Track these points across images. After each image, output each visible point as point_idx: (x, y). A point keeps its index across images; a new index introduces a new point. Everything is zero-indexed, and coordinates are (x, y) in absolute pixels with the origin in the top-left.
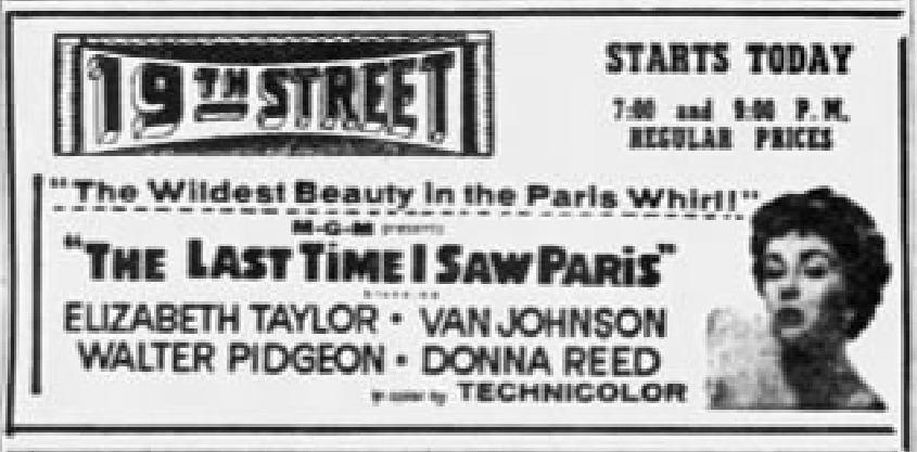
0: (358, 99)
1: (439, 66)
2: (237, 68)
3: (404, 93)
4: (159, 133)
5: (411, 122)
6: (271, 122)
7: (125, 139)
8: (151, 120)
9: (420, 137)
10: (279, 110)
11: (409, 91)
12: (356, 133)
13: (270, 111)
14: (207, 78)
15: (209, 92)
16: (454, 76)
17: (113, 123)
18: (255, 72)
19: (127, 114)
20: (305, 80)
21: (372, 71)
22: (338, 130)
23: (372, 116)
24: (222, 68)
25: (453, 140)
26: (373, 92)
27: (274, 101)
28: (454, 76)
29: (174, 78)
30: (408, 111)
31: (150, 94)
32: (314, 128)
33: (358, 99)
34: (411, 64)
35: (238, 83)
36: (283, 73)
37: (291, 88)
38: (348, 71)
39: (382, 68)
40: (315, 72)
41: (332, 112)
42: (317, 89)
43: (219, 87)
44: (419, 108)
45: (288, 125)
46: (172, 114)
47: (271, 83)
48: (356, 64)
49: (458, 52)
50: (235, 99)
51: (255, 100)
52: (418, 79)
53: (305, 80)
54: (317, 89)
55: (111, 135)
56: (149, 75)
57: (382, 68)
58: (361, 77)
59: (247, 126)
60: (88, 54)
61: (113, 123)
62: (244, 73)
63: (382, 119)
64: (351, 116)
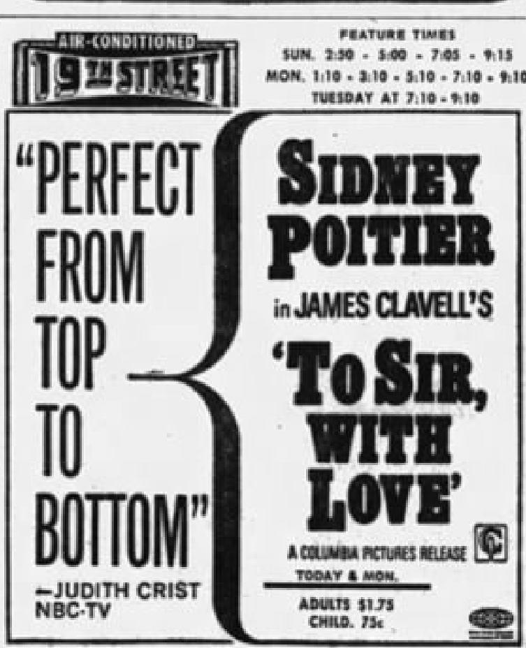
0: (171, 79)
1: (211, 60)
2: (107, 60)
3: (194, 74)
4: (67, 94)
5: (196, 90)
6: (124, 89)
7: (51, 97)
8: (64, 87)
9: (201, 98)
12: (167, 96)
13: (122, 84)
14: (92, 65)
16: (219, 66)
18: (115, 62)
19: (52, 85)
21: (177, 63)
22: (158, 93)
23: (177, 86)
24: (100, 60)
25: (218, 100)
28: (219, 66)
29: (76, 64)
31: (63, 73)
32: (146, 92)
35: (107, 69)
36: (129, 64)
37: (133, 71)
38: (164, 63)
40: (146, 63)
41: (155, 84)
42: (147, 73)
43: (98, 71)
44: (201, 83)
45: (133, 92)
46: (75, 85)
47: (124, 68)
48: (168, 58)
49: (220, 53)
50: (105, 77)
52: (201, 68)
53: (141, 66)
54: (147, 73)
55: (43, 96)
56: (63, 62)
59: (111, 91)
60: (32, 52)
61: (44, 88)
62: (110, 64)
64: (165, 86)
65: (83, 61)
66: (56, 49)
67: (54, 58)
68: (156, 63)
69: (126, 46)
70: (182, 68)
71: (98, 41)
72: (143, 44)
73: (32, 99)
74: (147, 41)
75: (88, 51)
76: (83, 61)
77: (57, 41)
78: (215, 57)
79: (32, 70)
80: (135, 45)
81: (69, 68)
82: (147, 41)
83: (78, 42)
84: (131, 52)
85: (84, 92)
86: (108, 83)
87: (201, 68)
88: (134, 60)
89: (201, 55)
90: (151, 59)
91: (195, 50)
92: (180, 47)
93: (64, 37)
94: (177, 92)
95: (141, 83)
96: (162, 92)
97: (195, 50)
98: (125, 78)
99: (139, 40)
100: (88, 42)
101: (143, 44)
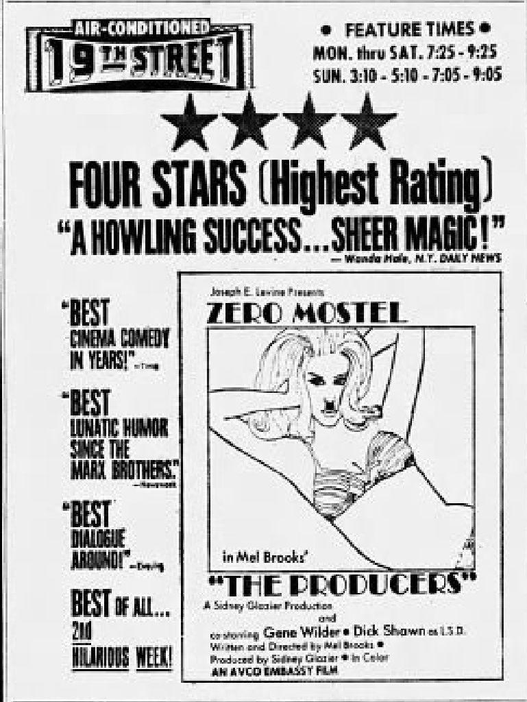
0: (184, 62)
1: (225, 42)
2: (120, 45)
3: (207, 57)
4: (82, 80)
5: (211, 73)
6: (139, 73)
7: (65, 82)
8: (78, 72)
9: (216, 80)
10: (142, 67)
11: (210, 57)
12: (183, 79)
13: (137, 68)
14: (106, 50)
15: (107, 58)
16: (233, 48)
17: (59, 74)
18: (129, 47)
19: (66, 70)
20: (155, 50)
21: (191, 46)
22: (174, 77)
23: (192, 69)
24: (113, 46)
25: (233, 82)
26: (192, 57)
27: (139, 62)
28: (233, 48)
29: (90, 50)
30: (209, 66)
31: (78, 60)
32: (160, 76)
33: (184, 62)
34: (211, 42)
35: (121, 53)
36: (144, 49)
37: (148, 55)
38: (179, 47)
39: (196, 44)
40: (162, 48)
41: (171, 67)
42: (162, 56)
43: (112, 55)
44: (216, 64)
45: (146, 76)
46: (89, 70)
47: (138, 53)
48: (183, 42)
49: (234, 35)
50: (120, 61)
51: (130, 62)
52: (215, 50)
53: (155, 50)
54: (162, 56)
55: (58, 81)
56: (78, 49)
57: (196, 44)
58: (185, 52)
59: (124, 75)
60: (44, 39)
61: (59, 74)
62: (123, 48)
63: (196, 71)
64: (180, 69)
65: (97, 46)
66: (71, 36)
67: (68, 45)
68: (170, 47)
69: (141, 33)
70: (197, 51)
71: (114, 28)
72: (158, 32)
73: (45, 86)
74: (162, 27)
75: (104, 37)
76: (97, 46)
77: (73, 28)
78: (230, 39)
79: (45, 55)
80: (151, 32)
81: (83, 54)
82: (162, 27)
83: (95, 29)
84: (146, 38)
85: (98, 77)
86: (123, 66)
87: (215, 50)
88: (148, 45)
89: (215, 38)
90: (165, 44)
91: (211, 33)
92: (196, 32)
93: (80, 24)
94: (192, 75)
95: (156, 67)
96: (178, 76)
97: (211, 33)
98: (139, 62)
99: (154, 27)
100: (104, 30)
101: (158, 32)
